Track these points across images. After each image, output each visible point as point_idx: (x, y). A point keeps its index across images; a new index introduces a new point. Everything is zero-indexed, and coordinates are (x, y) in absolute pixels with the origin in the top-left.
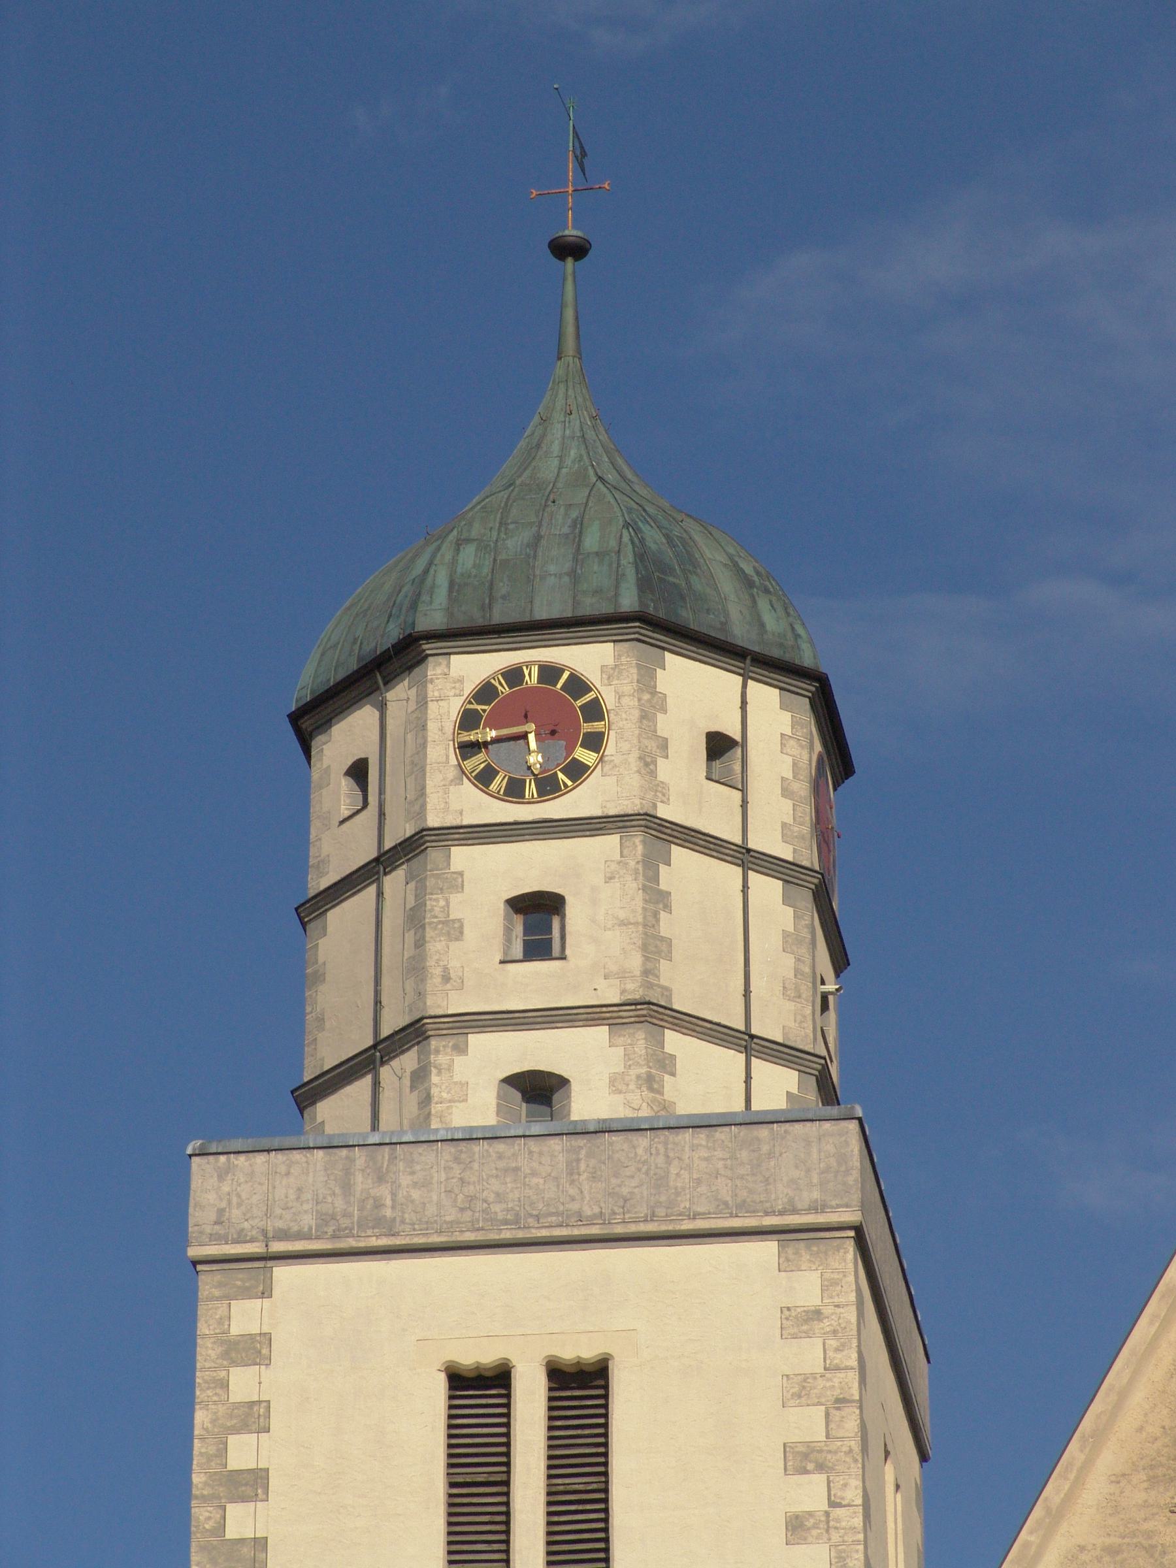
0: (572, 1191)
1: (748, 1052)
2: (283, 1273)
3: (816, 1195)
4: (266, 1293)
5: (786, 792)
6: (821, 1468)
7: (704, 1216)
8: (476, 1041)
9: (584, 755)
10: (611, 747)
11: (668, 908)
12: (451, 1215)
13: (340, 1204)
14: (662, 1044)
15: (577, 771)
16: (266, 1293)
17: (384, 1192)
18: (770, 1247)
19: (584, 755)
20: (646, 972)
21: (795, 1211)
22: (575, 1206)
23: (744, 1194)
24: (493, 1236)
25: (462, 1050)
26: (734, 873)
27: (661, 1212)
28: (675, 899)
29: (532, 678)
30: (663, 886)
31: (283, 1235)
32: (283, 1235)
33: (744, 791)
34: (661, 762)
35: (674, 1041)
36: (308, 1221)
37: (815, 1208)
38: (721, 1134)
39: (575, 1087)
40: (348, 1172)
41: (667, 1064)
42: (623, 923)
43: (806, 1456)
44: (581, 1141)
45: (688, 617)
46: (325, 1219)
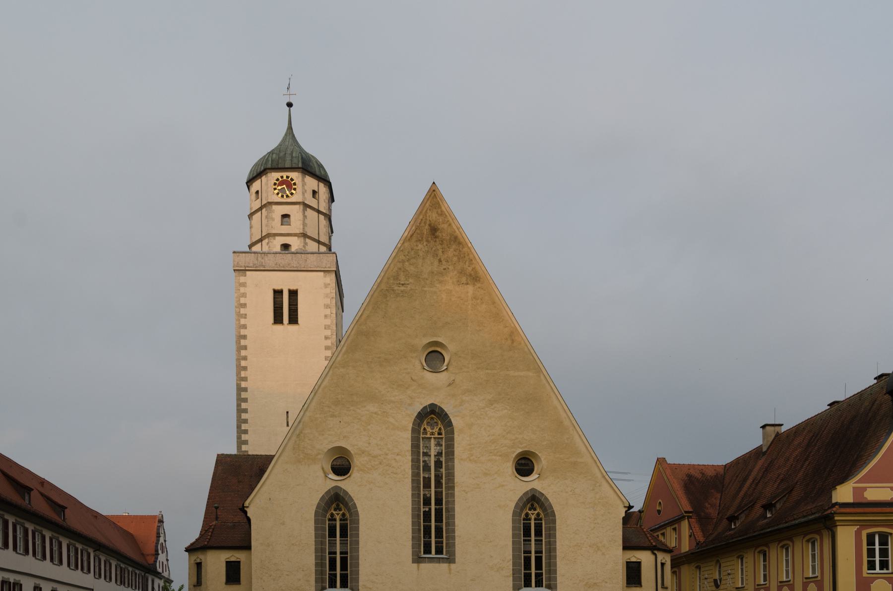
1: (319, 241)
2: (248, 273)
3: (329, 265)
4: (245, 276)
6: (330, 308)
8: (277, 238)
12: (274, 265)
13: (256, 262)
16: (245, 276)
17: (263, 261)
18: (322, 273)
20: (303, 229)
21: (326, 268)
24: (280, 269)
25: (274, 239)
31: (248, 267)
32: (248, 267)
35: (308, 240)
36: (251, 265)
38: (315, 255)
39: (292, 247)
40: (257, 257)
41: (306, 244)
43: (327, 306)
44: (293, 255)
46: (254, 264)
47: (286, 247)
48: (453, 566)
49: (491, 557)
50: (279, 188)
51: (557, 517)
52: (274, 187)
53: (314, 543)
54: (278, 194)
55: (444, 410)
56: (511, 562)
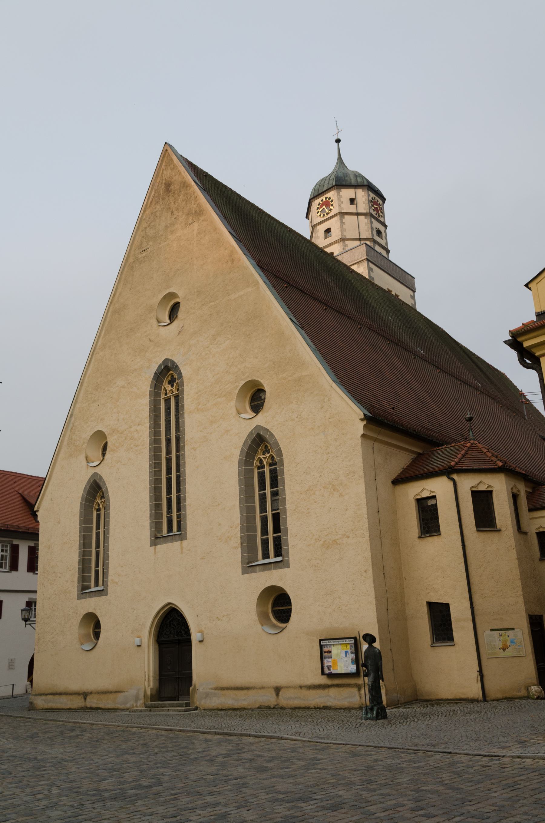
5: (364, 203)
9: (331, 207)
10: (335, 205)
11: (344, 224)
14: (345, 243)
15: (331, 210)
19: (331, 207)
21: (358, 259)
26: (356, 217)
29: (324, 200)
30: (343, 222)
33: (357, 205)
34: (342, 205)
37: (361, 258)
42: (338, 228)
45: (344, 183)
48: (185, 543)
49: (220, 524)
50: (321, 210)
51: (284, 457)
52: (317, 211)
54: (320, 215)
55: (175, 363)
56: (239, 528)
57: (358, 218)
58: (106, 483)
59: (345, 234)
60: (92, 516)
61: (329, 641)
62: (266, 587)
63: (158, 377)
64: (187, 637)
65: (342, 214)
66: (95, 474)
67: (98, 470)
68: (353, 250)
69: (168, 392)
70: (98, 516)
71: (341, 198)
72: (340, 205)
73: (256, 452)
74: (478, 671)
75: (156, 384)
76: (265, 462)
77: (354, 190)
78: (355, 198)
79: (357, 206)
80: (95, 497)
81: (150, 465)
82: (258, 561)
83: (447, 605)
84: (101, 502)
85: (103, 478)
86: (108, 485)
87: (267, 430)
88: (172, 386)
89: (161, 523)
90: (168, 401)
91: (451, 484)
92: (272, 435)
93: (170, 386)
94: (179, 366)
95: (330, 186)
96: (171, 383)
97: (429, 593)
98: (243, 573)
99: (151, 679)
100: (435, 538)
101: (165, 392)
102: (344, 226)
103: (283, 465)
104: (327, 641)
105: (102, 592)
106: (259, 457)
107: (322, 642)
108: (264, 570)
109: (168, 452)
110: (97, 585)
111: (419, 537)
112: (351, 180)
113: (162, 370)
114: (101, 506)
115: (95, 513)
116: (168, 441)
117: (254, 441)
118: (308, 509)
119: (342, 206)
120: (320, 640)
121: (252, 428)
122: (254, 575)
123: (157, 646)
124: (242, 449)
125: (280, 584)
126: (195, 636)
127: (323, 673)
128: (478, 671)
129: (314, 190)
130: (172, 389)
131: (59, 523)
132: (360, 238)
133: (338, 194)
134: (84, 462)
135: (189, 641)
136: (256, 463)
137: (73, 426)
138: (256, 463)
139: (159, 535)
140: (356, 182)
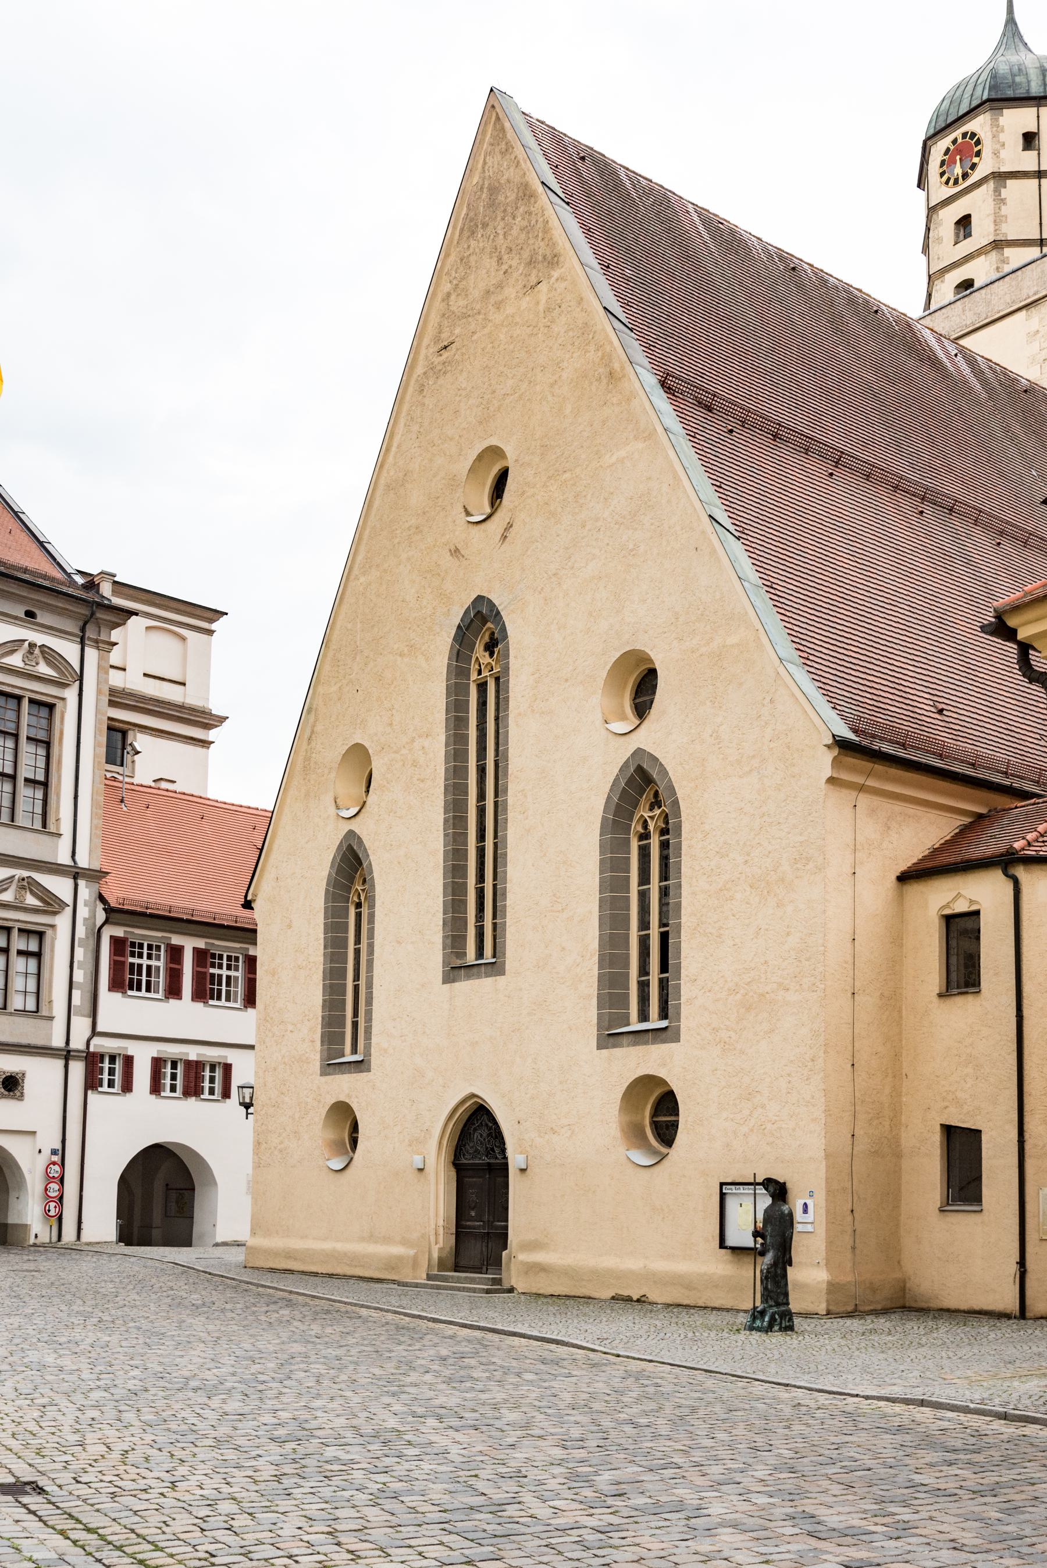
0: (964, 317)
7: (1002, 310)
10: (984, 154)
18: (1024, 312)
22: (964, 323)
23: (1014, 297)
27: (989, 314)
28: (1008, 201)
33: (1039, 150)
34: (1002, 152)
42: (988, 216)
47: (967, 285)
49: (563, 949)
52: (941, 170)
53: (322, 959)
54: (947, 183)
56: (596, 958)
57: (1040, 185)
58: (370, 852)
59: (1003, 231)
60: (347, 917)
61: (737, 1187)
62: (636, 1076)
63: (463, 637)
64: (503, 1161)
65: (1001, 177)
66: (351, 834)
67: (354, 826)
68: (1019, 272)
69: (483, 667)
70: (359, 916)
71: (1001, 134)
72: (996, 154)
73: (635, 805)
74: (1017, 1263)
75: (459, 651)
76: (651, 826)
77: (1036, 108)
78: (1036, 131)
79: (1039, 154)
80: (351, 880)
81: (446, 821)
82: (628, 1024)
83: (978, 1132)
84: (363, 890)
85: (365, 842)
86: (371, 858)
87: (654, 759)
88: (491, 655)
89: (464, 938)
90: (482, 687)
91: (1009, 888)
92: (664, 772)
93: (487, 654)
94: (502, 613)
95: (975, 103)
96: (490, 647)
97: (946, 1107)
98: (600, 1047)
99: (441, 1231)
100: (970, 998)
101: (477, 667)
102: (1003, 208)
103: (680, 835)
104: (733, 1187)
105: (361, 1066)
106: (642, 816)
107: (724, 1187)
108: (635, 1044)
109: (481, 796)
110: (354, 1051)
111: (940, 995)
112: (1029, 82)
113: (472, 621)
114: (362, 898)
115: (352, 911)
116: (482, 771)
117: (630, 782)
118: (721, 928)
119: (1003, 154)
120: (722, 1184)
121: (628, 754)
122: (617, 1052)
123: (453, 1174)
124: (609, 798)
125: (662, 1073)
126: (515, 1159)
127: (722, 1245)
128: (1017, 1263)
129: (937, 114)
130: (490, 661)
131: (290, 926)
132: (1042, 240)
133: (995, 124)
134: (332, 809)
135: (505, 1167)
136: (636, 827)
137: (313, 732)
138: (636, 827)
139: (458, 963)
140: (1042, 90)
